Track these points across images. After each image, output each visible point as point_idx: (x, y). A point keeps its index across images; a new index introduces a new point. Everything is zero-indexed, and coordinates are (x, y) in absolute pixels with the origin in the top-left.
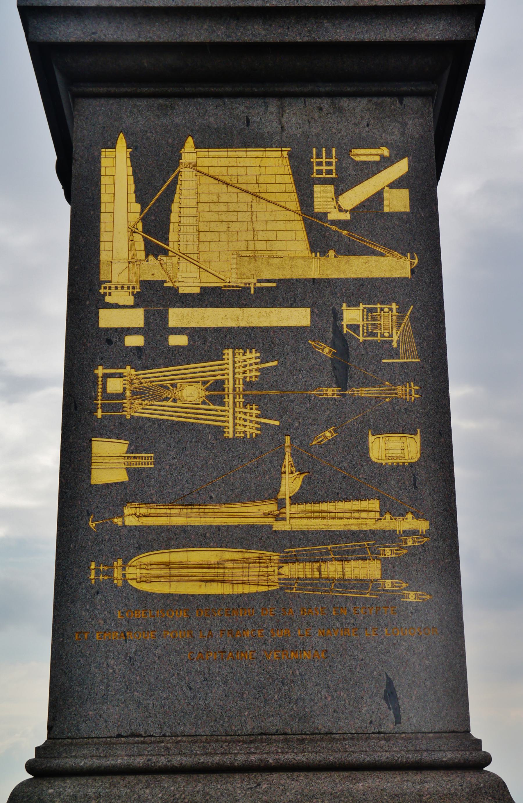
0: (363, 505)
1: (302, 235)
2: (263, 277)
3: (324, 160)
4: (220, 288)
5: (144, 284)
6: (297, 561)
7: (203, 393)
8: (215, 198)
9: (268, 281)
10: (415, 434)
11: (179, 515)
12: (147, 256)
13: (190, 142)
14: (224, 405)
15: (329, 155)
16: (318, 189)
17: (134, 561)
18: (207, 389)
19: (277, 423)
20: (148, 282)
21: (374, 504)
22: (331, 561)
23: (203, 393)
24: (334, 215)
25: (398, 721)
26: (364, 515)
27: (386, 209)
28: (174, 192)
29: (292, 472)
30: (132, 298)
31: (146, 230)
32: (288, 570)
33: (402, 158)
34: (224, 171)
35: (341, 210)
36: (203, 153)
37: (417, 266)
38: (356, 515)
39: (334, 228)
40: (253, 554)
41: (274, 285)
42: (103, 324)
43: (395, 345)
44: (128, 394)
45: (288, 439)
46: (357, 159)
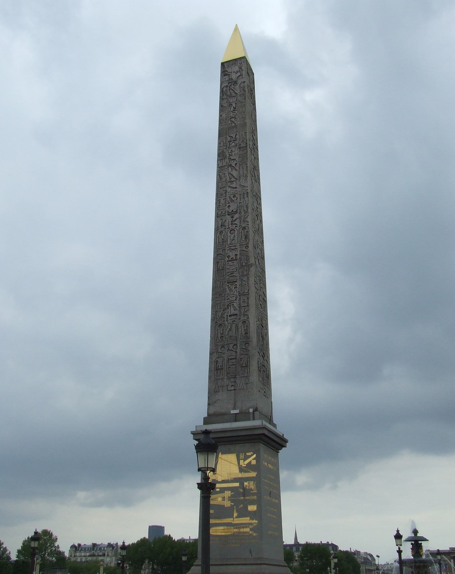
2: (232, 477)
3: (242, 455)
9: (232, 478)
11: (218, 521)
12: (213, 475)
13: (220, 453)
14: (225, 501)
15: (243, 454)
18: (223, 498)
19: (233, 504)
20: (213, 479)
25: (252, 556)
28: (218, 463)
32: (234, 530)
33: (255, 454)
35: (244, 464)
36: (222, 455)
40: (229, 527)
41: (233, 479)
43: (253, 489)
45: (235, 507)
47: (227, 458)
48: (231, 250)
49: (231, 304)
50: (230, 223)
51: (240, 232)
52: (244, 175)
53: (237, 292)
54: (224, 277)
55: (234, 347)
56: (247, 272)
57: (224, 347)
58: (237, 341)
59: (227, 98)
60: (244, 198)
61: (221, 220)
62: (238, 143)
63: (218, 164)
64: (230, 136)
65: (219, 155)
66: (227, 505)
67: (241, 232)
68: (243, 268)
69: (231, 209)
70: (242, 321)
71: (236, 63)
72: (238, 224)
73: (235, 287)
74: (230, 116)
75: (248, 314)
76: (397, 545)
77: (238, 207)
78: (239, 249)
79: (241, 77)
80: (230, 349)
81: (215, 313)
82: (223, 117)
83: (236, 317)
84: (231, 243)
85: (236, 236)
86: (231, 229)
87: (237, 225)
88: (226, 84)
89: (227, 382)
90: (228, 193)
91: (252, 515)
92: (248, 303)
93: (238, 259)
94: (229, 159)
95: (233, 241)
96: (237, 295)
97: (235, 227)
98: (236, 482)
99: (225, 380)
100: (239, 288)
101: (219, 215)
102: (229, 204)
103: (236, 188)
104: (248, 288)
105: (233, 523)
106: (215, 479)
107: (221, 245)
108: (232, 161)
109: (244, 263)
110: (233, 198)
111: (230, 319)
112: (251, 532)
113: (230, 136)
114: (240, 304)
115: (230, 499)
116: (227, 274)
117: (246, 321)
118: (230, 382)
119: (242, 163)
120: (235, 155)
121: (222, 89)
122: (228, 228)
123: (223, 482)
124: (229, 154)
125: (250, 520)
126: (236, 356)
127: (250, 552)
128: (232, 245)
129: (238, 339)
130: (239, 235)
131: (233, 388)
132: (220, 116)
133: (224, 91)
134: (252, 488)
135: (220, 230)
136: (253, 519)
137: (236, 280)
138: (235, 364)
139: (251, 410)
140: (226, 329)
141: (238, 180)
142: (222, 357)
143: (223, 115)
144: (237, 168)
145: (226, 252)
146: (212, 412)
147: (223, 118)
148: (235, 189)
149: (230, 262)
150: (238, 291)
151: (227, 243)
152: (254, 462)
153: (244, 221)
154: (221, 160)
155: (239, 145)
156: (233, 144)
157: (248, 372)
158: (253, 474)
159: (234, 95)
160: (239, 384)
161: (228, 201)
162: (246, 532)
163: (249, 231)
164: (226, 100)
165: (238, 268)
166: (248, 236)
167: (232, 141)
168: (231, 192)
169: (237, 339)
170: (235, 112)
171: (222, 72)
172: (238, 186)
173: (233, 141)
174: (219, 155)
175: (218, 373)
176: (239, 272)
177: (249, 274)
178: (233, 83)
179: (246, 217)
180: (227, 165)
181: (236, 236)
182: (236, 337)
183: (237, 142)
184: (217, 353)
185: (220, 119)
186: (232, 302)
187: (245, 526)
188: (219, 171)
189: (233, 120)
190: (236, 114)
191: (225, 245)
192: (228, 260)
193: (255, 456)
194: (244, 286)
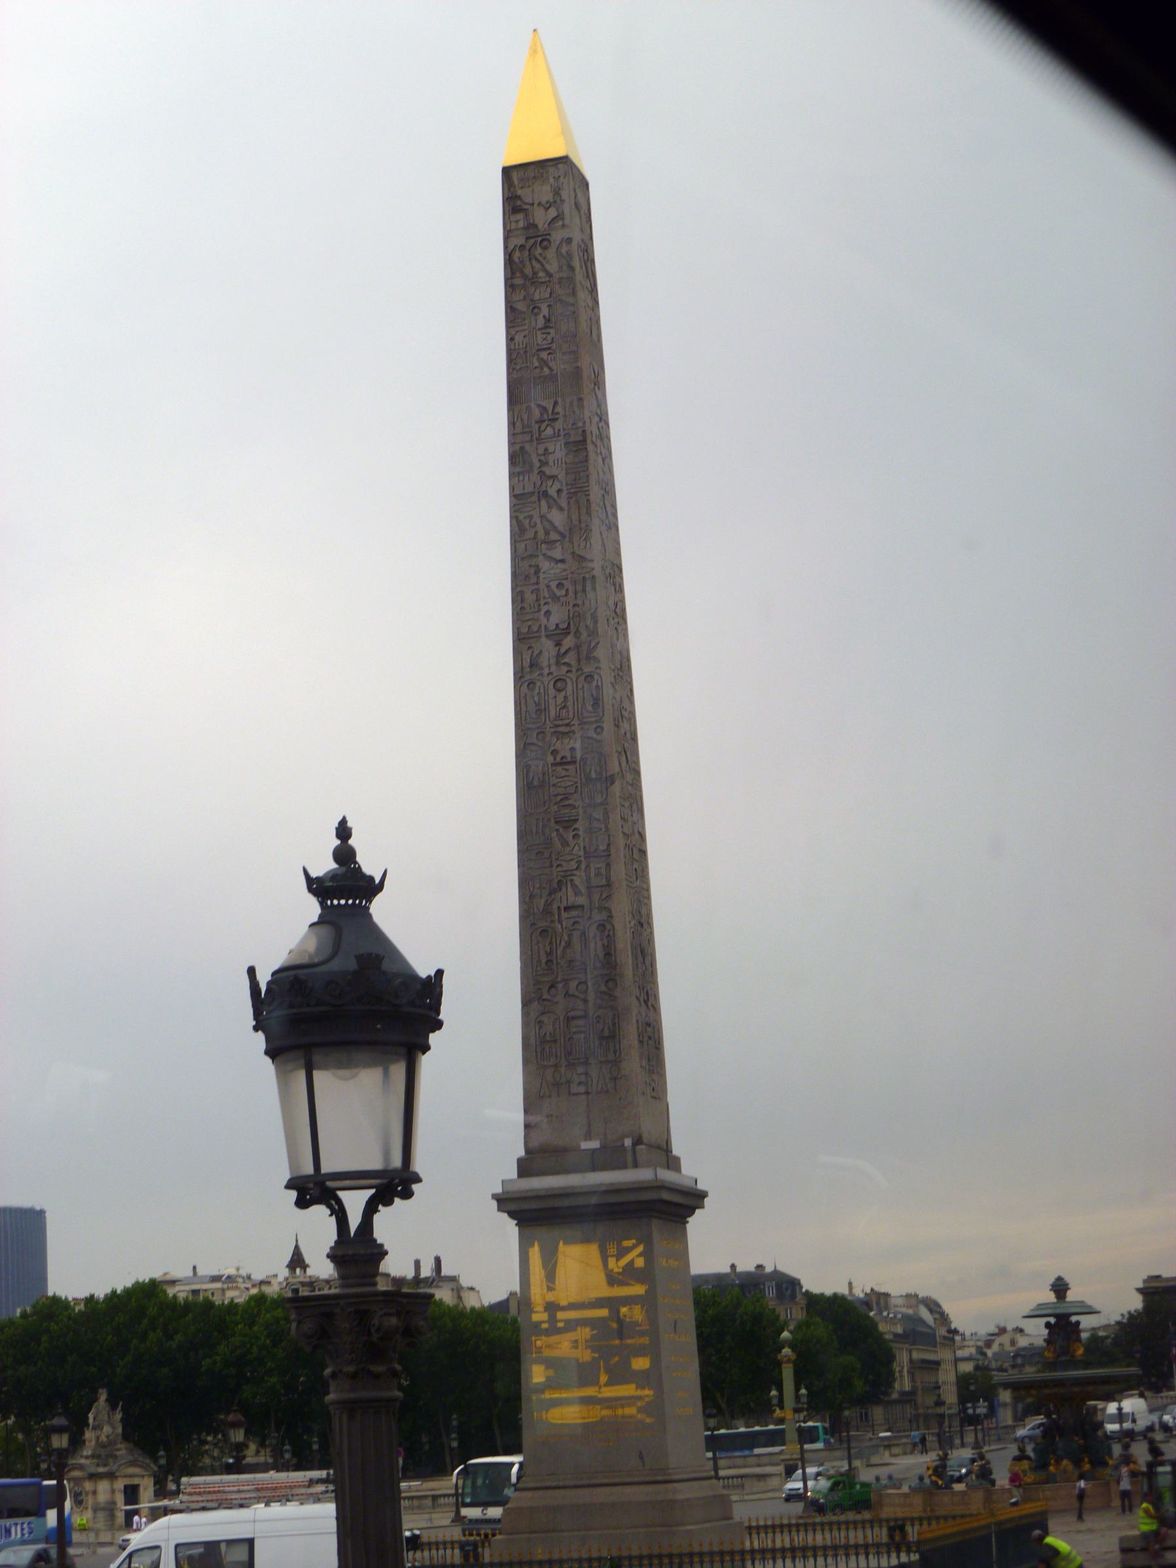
3: (611, 1246)
7: (572, 1345)
13: (561, 1242)
16: (610, 1259)
21: (633, 1386)
24: (616, 1270)
44: (544, 1346)
48: (561, 735)
50: (553, 661)
53: (580, 849)
54: (547, 807)
55: (580, 987)
56: (602, 796)
58: (586, 973)
59: (524, 287)
60: (584, 591)
61: (530, 652)
62: (562, 430)
64: (539, 406)
66: (584, 1359)
67: (583, 687)
72: (573, 663)
74: (538, 345)
77: (571, 616)
79: (560, 223)
81: (527, 898)
82: (519, 345)
86: (556, 678)
88: (520, 241)
90: (544, 576)
91: (642, 1380)
92: (608, 879)
94: (541, 473)
95: (564, 711)
97: (568, 672)
98: (602, 1307)
99: (563, 1070)
100: (584, 838)
103: (562, 561)
104: (607, 840)
108: (550, 483)
110: (556, 591)
112: (639, 1415)
113: (539, 406)
114: (588, 880)
119: (574, 488)
120: (556, 465)
121: (510, 255)
122: (548, 674)
123: (572, 1306)
124: (539, 460)
125: (637, 1388)
126: (585, 1011)
127: (641, 1457)
128: (561, 723)
130: (577, 694)
131: (582, 1089)
132: (510, 339)
135: (528, 677)
138: (584, 1029)
139: (628, 1142)
140: (558, 941)
141: (567, 539)
144: (564, 504)
145: (547, 739)
146: (534, 1144)
147: (517, 347)
148: (559, 565)
149: (559, 769)
151: (547, 715)
152: (640, 1263)
153: (588, 658)
154: (519, 474)
156: (549, 431)
158: (639, 1290)
159: (543, 280)
160: (597, 1078)
161: (544, 598)
162: (631, 1417)
165: (579, 785)
166: (599, 700)
169: (586, 969)
170: (549, 333)
171: (505, 199)
172: (568, 557)
173: (549, 420)
176: (582, 796)
178: (540, 239)
180: (537, 491)
181: (570, 698)
183: (559, 425)
184: (540, 1001)
185: (511, 350)
186: (569, 873)
188: (517, 508)
189: (544, 355)
190: (553, 338)
193: (640, 1248)
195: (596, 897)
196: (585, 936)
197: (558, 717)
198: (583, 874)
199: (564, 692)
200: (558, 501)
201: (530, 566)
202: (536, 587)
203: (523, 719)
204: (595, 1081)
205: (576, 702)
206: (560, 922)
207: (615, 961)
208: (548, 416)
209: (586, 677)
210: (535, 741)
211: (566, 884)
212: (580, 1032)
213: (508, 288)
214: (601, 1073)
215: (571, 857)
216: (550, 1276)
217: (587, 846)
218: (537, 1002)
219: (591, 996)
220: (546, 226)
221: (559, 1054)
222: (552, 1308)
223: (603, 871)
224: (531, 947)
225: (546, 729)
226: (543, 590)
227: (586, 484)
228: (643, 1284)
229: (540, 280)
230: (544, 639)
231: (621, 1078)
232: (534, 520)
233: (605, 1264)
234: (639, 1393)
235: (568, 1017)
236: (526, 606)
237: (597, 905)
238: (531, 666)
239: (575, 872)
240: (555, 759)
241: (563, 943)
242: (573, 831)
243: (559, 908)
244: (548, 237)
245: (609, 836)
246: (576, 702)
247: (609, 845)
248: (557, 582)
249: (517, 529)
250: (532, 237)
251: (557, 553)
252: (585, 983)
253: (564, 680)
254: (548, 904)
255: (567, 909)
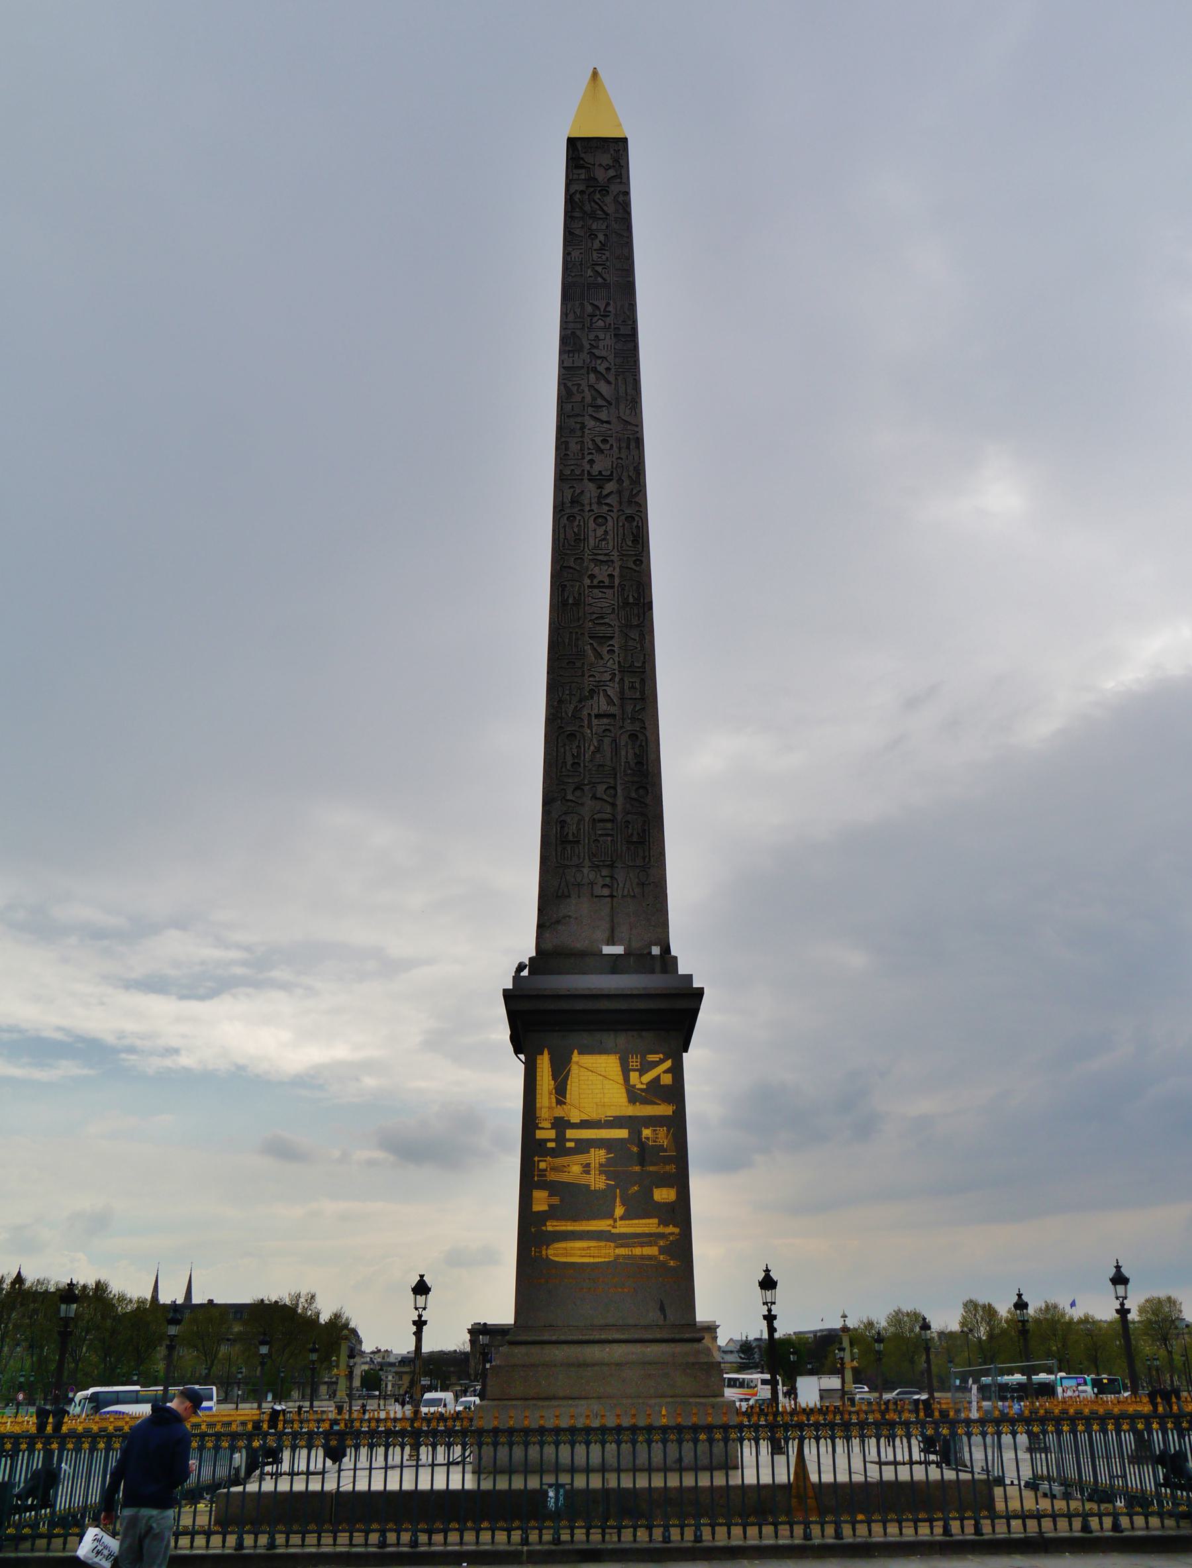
0: (651, 1221)
1: (625, 1095)
2: (608, 1115)
3: (634, 1060)
4: (588, 1120)
5: (555, 1118)
6: (622, 1247)
7: (581, 1169)
8: (586, 1078)
10: (674, 1188)
11: (571, 1226)
12: (557, 1105)
13: (576, 1051)
14: (590, 1174)
15: (637, 1058)
16: (632, 1074)
17: (551, 1247)
18: (583, 1167)
19: (613, 1183)
21: (656, 1221)
22: (637, 1246)
23: (581, 1169)
24: (639, 1086)
25: (665, 1320)
26: (651, 1226)
27: (662, 1083)
28: (569, 1076)
29: (620, 1206)
30: (550, 1125)
31: (556, 1093)
33: (669, 1059)
34: (590, 1065)
37: (676, 1110)
38: (648, 1226)
39: (639, 1092)
40: (602, 1244)
42: (537, 1137)
43: (665, 1146)
44: (548, 1169)
46: (649, 1059)
47: (594, 1065)
48: (598, 563)
49: (600, 688)
50: (594, 500)
51: (621, 524)
52: (629, 398)
54: (581, 622)
55: (608, 792)
56: (639, 620)
57: (583, 790)
58: (615, 778)
60: (628, 448)
61: (572, 490)
63: (563, 361)
64: (591, 304)
65: (565, 341)
67: (624, 525)
68: (628, 609)
69: (596, 468)
70: (629, 733)
71: (606, 147)
73: (610, 650)
74: (593, 260)
75: (643, 719)
76: (764, 1304)
77: (614, 466)
78: (617, 564)
80: (598, 796)
83: (612, 720)
84: (598, 547)
85: (611, 533)
87: (613, 507)
89: (590, 876)
90: (589, 432)
92: (643, 692)
93: (616, 587)
95: (604, 543)
96: (614, 670)
99: (586, 871)
100: (619, 654)
101: (565, 477)
102: (590, 457)
103: (608, 422)
104: (642, 658)
105: (612, 1232)
106: (563, 1116)
107: (570, 548)
108: (599, 362)
109: (631, 597)
111: (598, 723)
112: (662, 1256)
113: (591, 304)
114: (622, 692)
115: (604, 1169)
116: (587, 615)
117: (639, 735)
118: (598, 876)
120: (606, 349)
121: (571, 196)
122: (589, 511)
123: (585, 1124)
125: (659, 1225)
126: (613, 815)
128: (600, 552)
129: (618, 774)
132: (566, 254)
133: (574, 200)
134: (663, 1145)
135: (568, 511)
136: (666, 1225)
137: (612, 635)
138: (611, 833)
139: (656, 950)
141: (613, 405)
142: (575, 813)
143: (572, 253)
144: (612, 379)
145: (585, 564)
146: (548, 946)
148: (605, 425)
149: (596, 591)
150: (616, 659)
151: (586, 545)
152: (667, 1079)
154: (569, 352)
155: (615, 328)
156: (601, 323)
157: (646, 856)
158: (665, 1110)
159: (601, 217)
160: (624, 882)
161: (589, 449)
162: (650, 1258)
163: (643, 526)
164: (581, 223)
165: (616, 608)
167: (596, 316)
168: (596, 429)
169: (616, 774)
170: (604, 254)
171: (569, 157)
172: (614, 420)
174: (564, 340)
175: (567, 851)
176: (618, 616)
177: (644, 626)
178: (599, 188)
179: (635, 494)
181: (611, 533)
182: (614, 769)
183: (608, 320)
187: (645, 1240)
191: (582, 549)
192: (589, 584)
194: (632, 652)
195: (629, 709)
196: (616, 742)
197: (596, 547)
198: (617, 686)
199: (604, 527)
200: (606, 376)
201: (576, 423)
202: (581, 439)
203: (561, 545)
204: (621, 885)
205: (616, 536)
206: (590, 726)
207: (647, 769)
208: (600, 312)
209: (627, 518)
210: (572, 564)
211: (599, 693)
212: (607, 835)
213: (567, 218)
214: (628, 878)
215: (606, 669)
216: (561, 1091)
217: (622, 661)
218: (559, 802)
219: (620, 801)
220: (606, 180)
221: (583, 854)
222: (561, 1124)
223: (637, 686)
224: (557, 747)
225: (584, 555)
226: (588, 443)
227: (633, 367)
228: (669, 1104)
229: (598, 216)
230: (586, 481)
231: (650, 884)
232: (581, 388)
233: (626, 1079)
234: (661, 1230)
235: (594, 819)
236: (569, 453)
237: (630, 716)
238: (572, 502)
239: (608, 683)
240: (592, 582)
241: (592, 748)
242: (608, 646)
243: (589, 714)
244: (607, 188)
245: (645, 654)
246: (616, 536)
247: (644, 662)
248: (602, 438)
249: (564, 393)
250: (592, 187)
251: (603, 416)
252: (614, 788)
253: (606, 518)
254: (577, 710)
255: (598, 716)
